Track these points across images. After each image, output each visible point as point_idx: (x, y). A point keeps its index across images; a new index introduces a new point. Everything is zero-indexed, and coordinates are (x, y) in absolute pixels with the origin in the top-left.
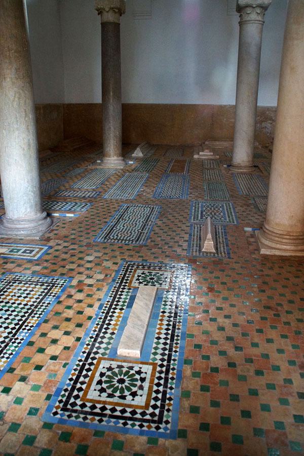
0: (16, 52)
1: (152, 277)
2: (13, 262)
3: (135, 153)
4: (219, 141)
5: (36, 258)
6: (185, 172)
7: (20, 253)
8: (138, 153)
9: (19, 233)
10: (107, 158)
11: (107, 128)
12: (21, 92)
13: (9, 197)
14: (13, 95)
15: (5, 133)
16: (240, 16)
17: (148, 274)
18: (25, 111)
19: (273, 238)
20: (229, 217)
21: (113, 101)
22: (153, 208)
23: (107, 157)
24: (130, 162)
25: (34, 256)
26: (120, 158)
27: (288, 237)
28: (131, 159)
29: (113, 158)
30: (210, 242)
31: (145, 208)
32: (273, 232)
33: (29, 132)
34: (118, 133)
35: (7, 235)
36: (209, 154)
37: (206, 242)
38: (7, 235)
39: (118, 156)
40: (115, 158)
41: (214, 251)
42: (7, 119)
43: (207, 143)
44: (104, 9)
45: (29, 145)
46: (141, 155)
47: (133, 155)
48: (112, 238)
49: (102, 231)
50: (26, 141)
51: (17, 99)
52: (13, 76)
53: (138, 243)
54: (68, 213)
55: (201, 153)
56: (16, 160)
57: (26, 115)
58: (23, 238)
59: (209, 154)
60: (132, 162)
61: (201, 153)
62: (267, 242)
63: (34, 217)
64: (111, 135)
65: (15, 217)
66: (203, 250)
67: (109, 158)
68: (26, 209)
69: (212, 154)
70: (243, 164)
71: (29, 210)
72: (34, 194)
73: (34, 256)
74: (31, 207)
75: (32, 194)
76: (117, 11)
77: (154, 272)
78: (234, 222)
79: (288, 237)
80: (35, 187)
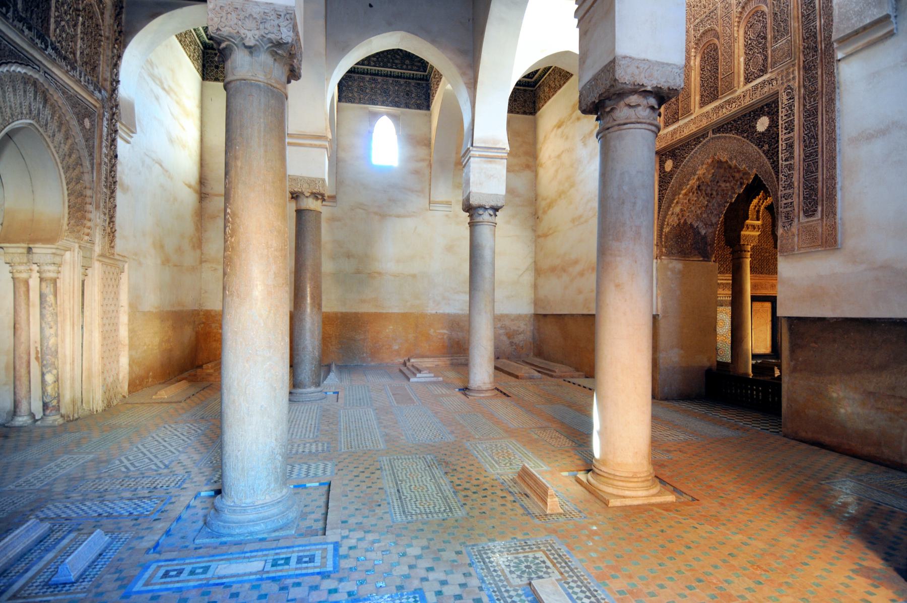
2: (298, 584)
9: (258, 528)
16: (471, 216)
19: (615, 483)
21: (312, 310)
23: (299, 388)
27: (636, 480)
29: (309, 390)
35: (232, 535)
37: (549, 500)
38: (232, 535)
43: (412, 360)
44: (302, 193)
48: (414, 512)
54: (310, 482)
58: (265, 536)
74: (276, 480)
75: (280, 458)
76: (320, 197)
79: (636, 480)
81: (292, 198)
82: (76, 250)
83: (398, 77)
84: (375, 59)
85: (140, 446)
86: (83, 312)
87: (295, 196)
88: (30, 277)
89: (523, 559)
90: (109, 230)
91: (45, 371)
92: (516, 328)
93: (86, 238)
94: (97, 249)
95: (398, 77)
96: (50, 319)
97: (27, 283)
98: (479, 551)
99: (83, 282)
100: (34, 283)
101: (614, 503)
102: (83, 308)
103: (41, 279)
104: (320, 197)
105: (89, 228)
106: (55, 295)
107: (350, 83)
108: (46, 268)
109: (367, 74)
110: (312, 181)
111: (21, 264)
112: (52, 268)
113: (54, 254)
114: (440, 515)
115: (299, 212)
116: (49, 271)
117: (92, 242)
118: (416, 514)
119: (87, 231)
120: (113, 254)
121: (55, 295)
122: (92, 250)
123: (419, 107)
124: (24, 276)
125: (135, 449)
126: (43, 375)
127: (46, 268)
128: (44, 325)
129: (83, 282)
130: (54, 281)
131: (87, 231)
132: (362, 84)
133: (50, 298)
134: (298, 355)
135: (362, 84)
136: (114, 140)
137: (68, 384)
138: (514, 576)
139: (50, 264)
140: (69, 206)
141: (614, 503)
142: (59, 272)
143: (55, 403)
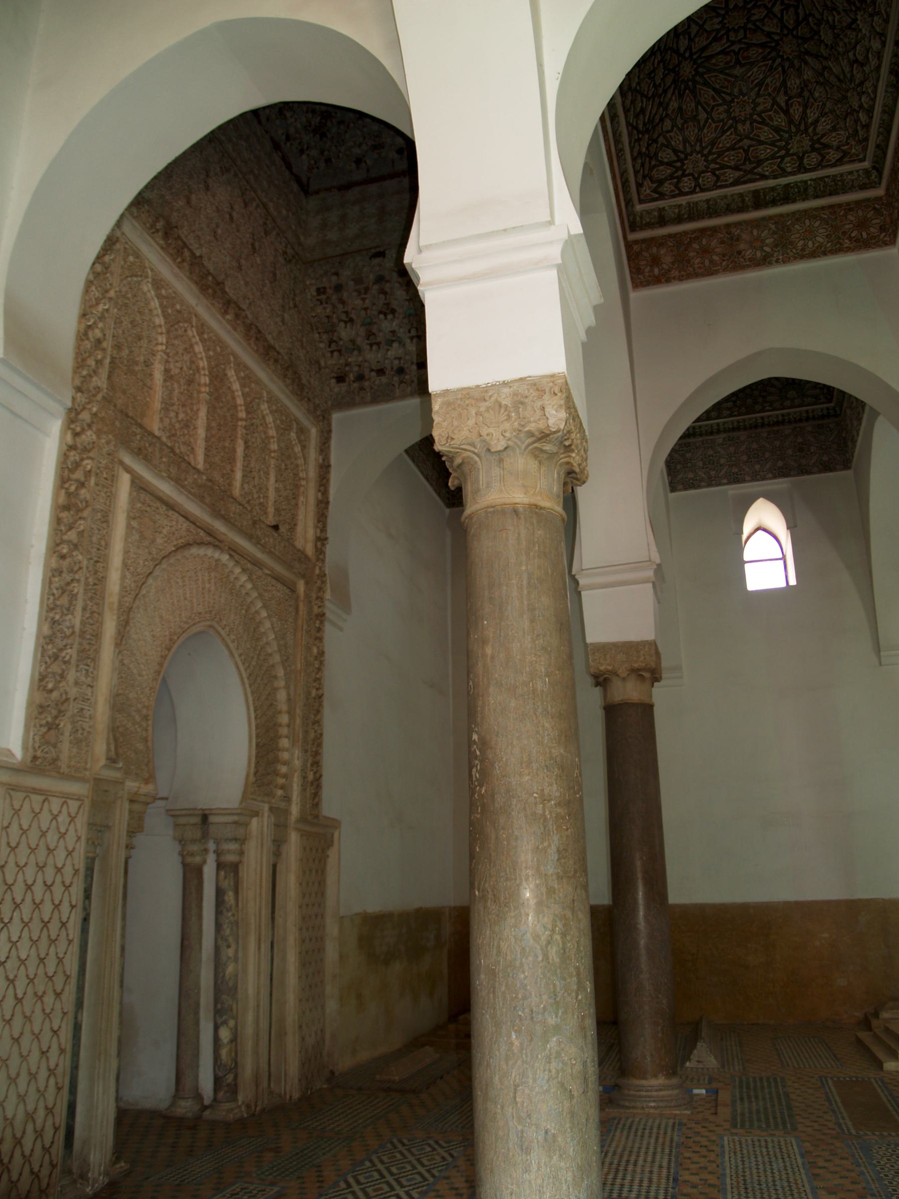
0: (558, 804)
8: (704, 1057)
12: (569, 914)
14: (550, 926)
15: (517, 1043)
18: (578, 974)
21: (647, 907)
26: (674, 1081)
33: (585, 1037)
40: (661, 1081)
42: (525, 998)
43: (885, 1015)
45: (585, 1080)
46: (712, 1062)
47: (688, 1064)
50: (578, 1067)
51: (558, 937)
52: (551, 871)
56: (546, 1132)
57: (580, 986)
60: (696, 1091)
76: (647, 675)
81: (597, 684)
82: (266, 814)
83: (778, 423)
84: (730, 404)
85: (351, 1180)
86: (273, 919)
87: (601, 681)
88: (205, 862)
91: (219, 1022)
93: (280, 792)
94: (295, 810)
95: (778, 423)
96: (228, 932)
97: (199, 871)
99: (274, 866)
100: (209, 870)
102: (273, 912)
103: (220, 866)
104: (647, 675)
105: (285, 776)
106: (237, 892)
107: (688, 455)
108: (227, 846)
109: (718, 432)
110: (628, 648)
111: (194, 841)
112: (233, 846)
113: (235, 823)
115: (612, 711)
116: (229, 851)
117: (287, 799)
119: (281, 781)
120: (317, 817)
121: (237, 892)
122: (287, 812)
123: (827, 467)
124: (198, 859)
125: (343, 1185)
126: (216, 1028)
127: (227, 846)
128: (220, 942)
129: (274, 866)
130: (235, 868)
131: (281, 781)
132: (710, 452)
133: (230, 897)
135: (710, 452)
136: (319, 630)
137: (249, 1045)
139: (231, 840)
140: (257, 745)
142: (242, 853)
143: (230, 1078)
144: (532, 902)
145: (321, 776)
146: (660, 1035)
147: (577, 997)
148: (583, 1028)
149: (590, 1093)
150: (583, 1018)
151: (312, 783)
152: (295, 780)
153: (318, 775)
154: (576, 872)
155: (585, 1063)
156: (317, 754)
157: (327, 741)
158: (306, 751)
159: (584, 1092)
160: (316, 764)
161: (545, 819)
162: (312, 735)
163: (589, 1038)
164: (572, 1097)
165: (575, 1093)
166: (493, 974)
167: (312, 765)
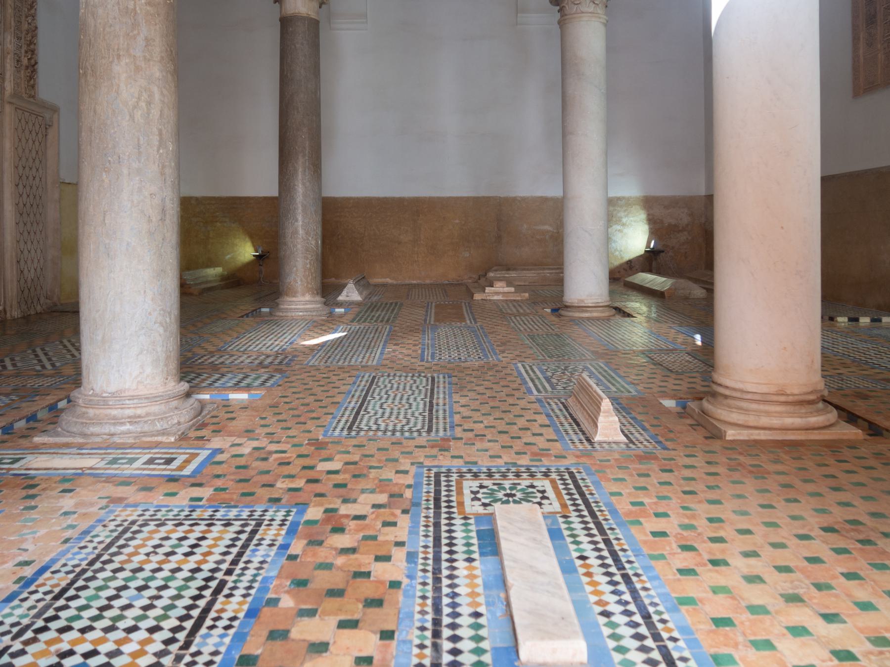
1: (508, 492)
3: (344, 293)
4: (515, 269)
5: (187, 471)
6: (468, 322)
7: (137, 464)
10: (288, 299)
11: (289, 232)
13: (99, 338)
17: (495, 487)
20: (613, 385)
22: (433, 379)
24: (337, 310)
25: (181, 468)
27: (782, 399)
28: (340, 305)
30: (611, 419)
31: (415, 378)
32: (742, 391)
34: (313, 242)
36: (507, 289)
39: (313, 293)
40: (308, 297)
41: (624, 439)
49: (334, 418)
53: (433, 434)
55: (488, 289)
59: (507, 289)
61: (488, 289)
62: (735, 417)
63: (161, 389)
64: (299, 246)
65: (112, 388)
66: (598, 438)
67: (294, 299)
68: (142, 367)
69: (512, 289)
70: (589, 302)
71: (149, 370)
72: (165, 331)
73: (181, 468)
75: (161, 330)
77: (507, 484)
78: (630, 392)
80: (170, 313)
89: (507, 486)
90: (25, 61)
92: (673, 222)
98: (437, 475)
101: (731, 434)
114: (407, 434)
118: (370, 429)
120: (33, 97)
134: (285, 244)
138: (477, 503)
141: (731, 434)
144: (123, 76)
145: (36, 63)
146: (308, 266)
147: (158, 151)
148: (162, 174)
149: (168, 221)
150: (164, 167)
151: (27, 68)
152: (8, 61)
153: (33, 62)
154: (162, 58)
155: (163, 200)
156: (31, 43)
157: (41, 32)
158: (19, 38)
159: (162, 220)
160: (32, 52)
161: (136, 13)
162: (25, 26)
163: (169, 183)
164: (150, 221)
165: (154, 219)
166: (91, 131)
167: (26, 52)
